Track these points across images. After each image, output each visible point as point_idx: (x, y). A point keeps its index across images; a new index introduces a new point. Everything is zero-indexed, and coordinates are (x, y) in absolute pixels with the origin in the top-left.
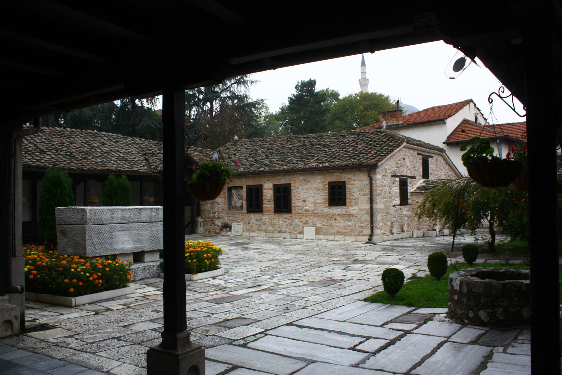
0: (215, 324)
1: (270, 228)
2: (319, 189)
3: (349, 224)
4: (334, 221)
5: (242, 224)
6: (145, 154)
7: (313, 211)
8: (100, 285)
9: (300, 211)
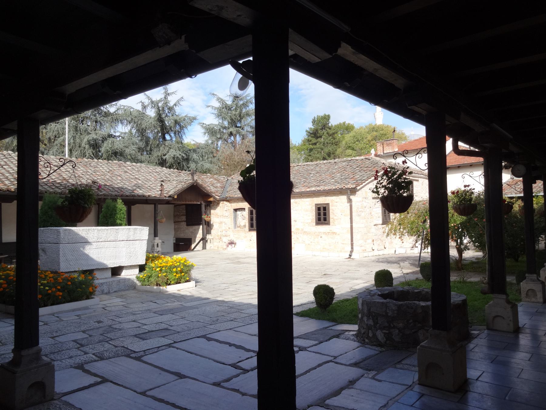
0: (136, 336)
6: (162, 181)
8: (60, 297)
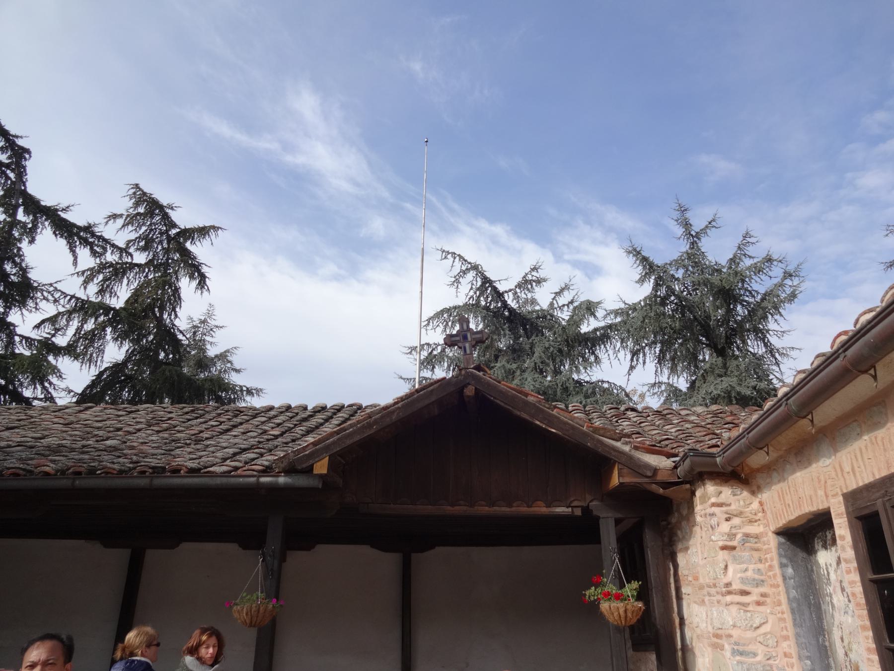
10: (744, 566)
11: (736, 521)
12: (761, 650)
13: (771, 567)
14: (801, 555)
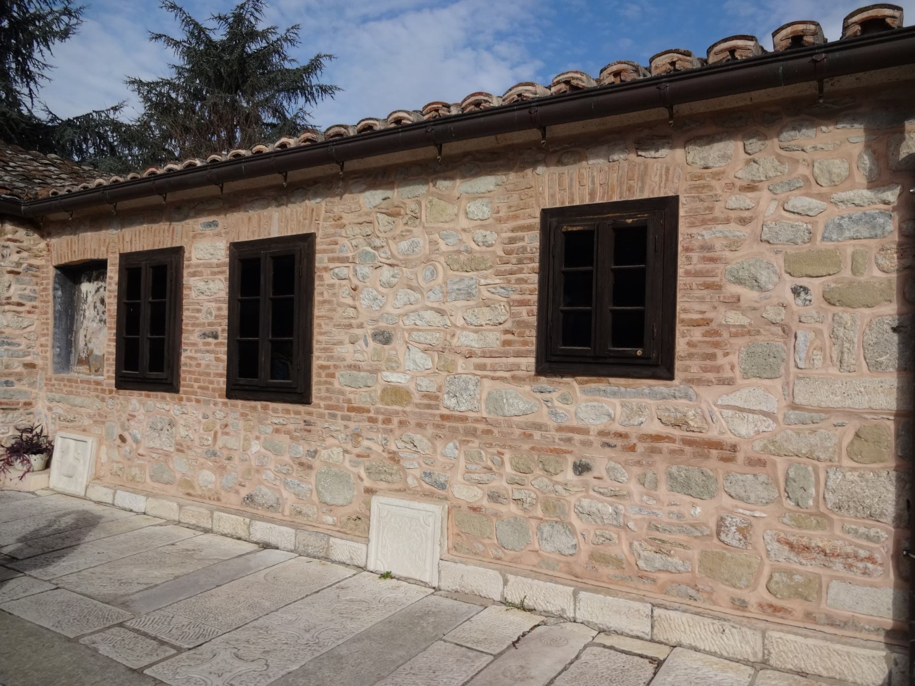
1: (207, 478)
2: (474, 264)
3: (699, 510)
4: (569, 475)
5: (91, 441)
7: (432, 400)
9: (360, 398)
10: (24, 286)
11: (25, 254)
12: (24, 343)
13: (45, 289)
14: (70, 283)
